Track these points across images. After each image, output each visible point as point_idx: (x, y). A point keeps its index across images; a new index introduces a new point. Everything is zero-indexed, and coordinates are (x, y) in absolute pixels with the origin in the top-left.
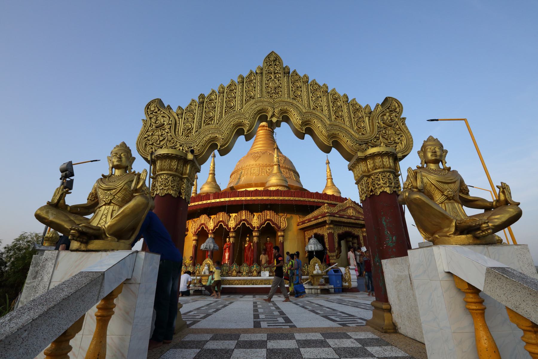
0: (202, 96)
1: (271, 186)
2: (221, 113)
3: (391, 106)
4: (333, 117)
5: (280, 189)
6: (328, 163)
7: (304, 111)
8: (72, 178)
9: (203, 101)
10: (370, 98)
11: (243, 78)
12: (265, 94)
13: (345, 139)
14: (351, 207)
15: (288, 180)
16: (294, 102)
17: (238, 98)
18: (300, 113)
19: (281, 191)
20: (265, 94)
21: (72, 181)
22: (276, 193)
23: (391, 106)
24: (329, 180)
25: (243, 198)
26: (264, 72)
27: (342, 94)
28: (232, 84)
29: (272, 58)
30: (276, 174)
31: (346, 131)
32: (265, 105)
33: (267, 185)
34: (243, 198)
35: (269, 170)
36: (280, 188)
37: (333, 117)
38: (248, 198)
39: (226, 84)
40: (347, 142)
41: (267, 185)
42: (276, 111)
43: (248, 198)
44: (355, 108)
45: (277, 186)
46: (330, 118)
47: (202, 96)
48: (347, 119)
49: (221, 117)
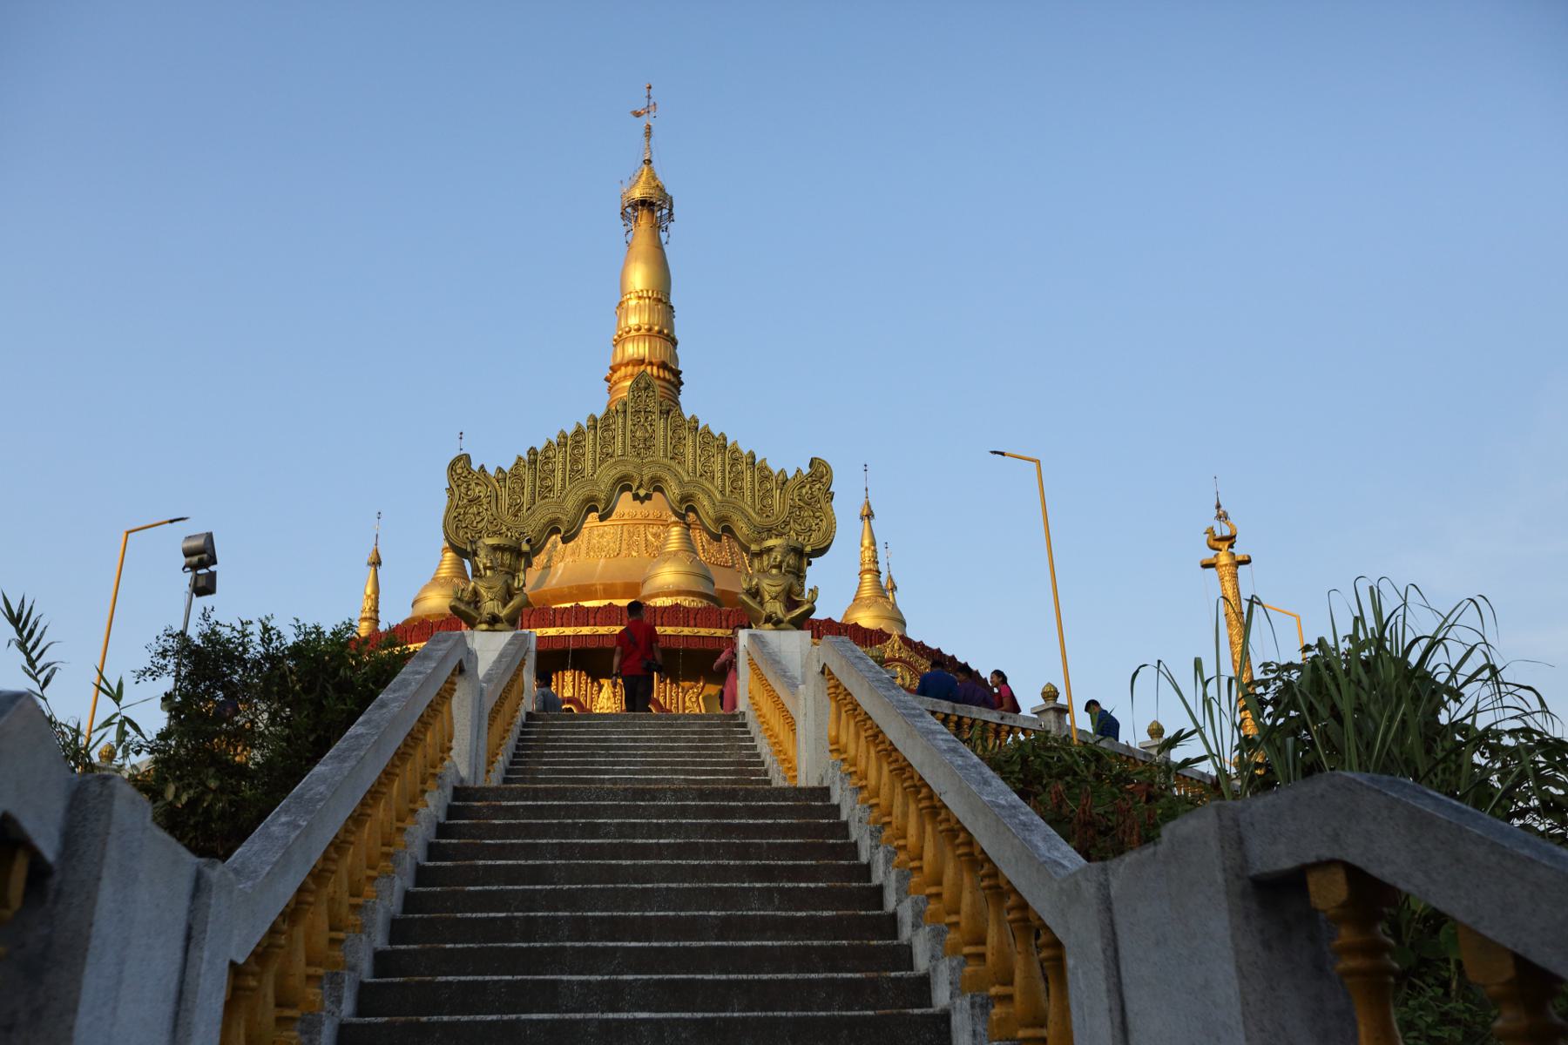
0: (533, 451)
1: (657, 595)
2: (563, 480)
3: (819, 472)
4: (728, 490)
5: (686, 604)
6: (869, 515)
7: (686, 479)
8: (212, 568)
9: (535, 460)
10: (787, 460)
11: (595, 420)
12: (629, 448)
13: (741, 524)
14: (900, 660)
15: (715, 573)
16: (673, 463)
17: (589, 456)
18: (681, 483)
19: (687, 610)
20: (629, 448)
21: (213, 575)
22: (674, 614)
23: (819, 472)
24: (868, 577)
25: (569, 631)
26: (629, 410)
27: (745, 452)
28: (579, 432)
29: (642, 385)
30: (676, 553)
31: (743, 512)
32: (629, 469)
33: (645, 591)
34: (569, 631)
35: (656, 536)
36: (685, 601)
37: (728, 490)
38: (586, 630)
39: (570, 431)
40: (742, 528)
41: (645, 591)
42: (646, 478)
43: (586, 630)
44: (764, 474)
45: (679, 593)
46: (722, 492)
47: (533, 451)
48: (748, 493)
49: (564, 486)
